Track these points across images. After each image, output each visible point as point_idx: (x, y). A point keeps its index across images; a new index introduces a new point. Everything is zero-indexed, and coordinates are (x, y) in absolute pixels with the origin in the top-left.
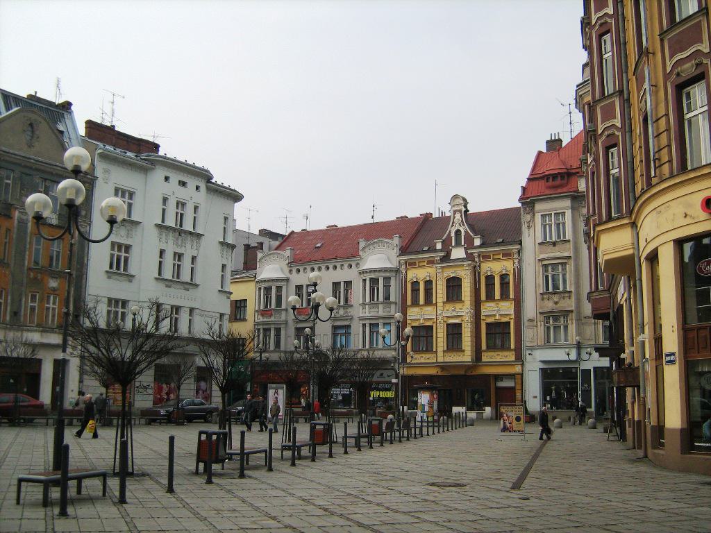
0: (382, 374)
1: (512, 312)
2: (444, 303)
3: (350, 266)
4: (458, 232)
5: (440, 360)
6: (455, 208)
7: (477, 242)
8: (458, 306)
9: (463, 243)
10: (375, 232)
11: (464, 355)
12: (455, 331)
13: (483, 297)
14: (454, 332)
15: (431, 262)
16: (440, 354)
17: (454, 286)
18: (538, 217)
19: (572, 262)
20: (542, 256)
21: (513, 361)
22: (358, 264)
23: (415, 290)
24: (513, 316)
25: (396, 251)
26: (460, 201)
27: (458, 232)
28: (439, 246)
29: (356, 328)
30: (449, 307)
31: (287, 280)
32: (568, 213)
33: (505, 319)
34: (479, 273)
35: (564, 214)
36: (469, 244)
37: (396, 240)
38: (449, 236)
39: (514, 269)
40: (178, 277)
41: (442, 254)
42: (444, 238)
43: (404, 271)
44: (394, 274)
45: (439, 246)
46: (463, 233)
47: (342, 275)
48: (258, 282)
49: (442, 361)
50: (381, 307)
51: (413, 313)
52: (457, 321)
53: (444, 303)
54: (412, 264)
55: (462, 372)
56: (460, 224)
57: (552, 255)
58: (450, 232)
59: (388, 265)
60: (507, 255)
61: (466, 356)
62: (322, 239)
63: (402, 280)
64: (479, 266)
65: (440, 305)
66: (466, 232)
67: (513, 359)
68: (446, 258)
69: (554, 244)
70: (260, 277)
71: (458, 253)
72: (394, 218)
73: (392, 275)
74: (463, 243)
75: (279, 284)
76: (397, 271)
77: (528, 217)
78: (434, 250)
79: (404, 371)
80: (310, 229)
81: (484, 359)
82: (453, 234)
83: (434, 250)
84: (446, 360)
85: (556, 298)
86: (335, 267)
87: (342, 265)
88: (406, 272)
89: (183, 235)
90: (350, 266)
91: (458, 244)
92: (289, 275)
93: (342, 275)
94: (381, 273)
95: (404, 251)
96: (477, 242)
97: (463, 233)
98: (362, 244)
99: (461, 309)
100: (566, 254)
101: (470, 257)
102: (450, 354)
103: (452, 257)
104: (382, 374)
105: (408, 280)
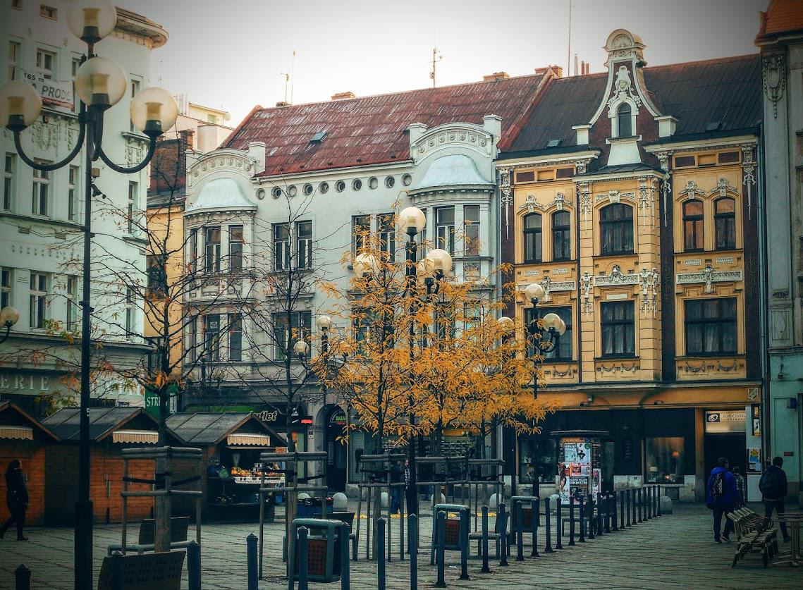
1: (741, 278)
2: (595, 258)
3: (390, 181)
4: (623, 110)
5: (588, 377)
6: (618, 59)
7: (666, 129)
8: (626, 263)
9: (634, 133)
10: (447, 108)
11: (638, 368)
12: (620, 315)
13: (679, 247)
14: (618, 320)
15: (566, 174)
16: (588, 366)
17: (617, 222)
21: (742, 380)
22: (407, 177)
23: (532, 233)
24: (741, 286)
25: (491, 149)
28: (583, 138)
30: (605, 264)
31: (253, 212)
33: (725, 293)
34: (670, 196)
36: (648, 129)
37: (493, 125)
38: (605, 119)
39: (745, 187)
40: (43, 211)
41: (592, 155)
42: (593, 121)
43: (507, 192)
44: (487, 197)
45: (583, 138)
46: (634, 112)
47: (374, 197)
48: (188, 217)
49: (593, 380)
51: (531, 284)
52: (623, 296)
53: (595, 258)
54: (527, 177)
55: (633, 403)
56: (627, 92)
58: (607, 109)
59: (473, 179)
60: (728, 158)
61: (647, 369)
62: (325, 122)
63: (503, 209)
64: (670, 181)
65: (586, 262)
66: (642, 109)
67: (742, 374)
68: (597, 166)
70: (189, 209)
71: (624, 153)
73: (481, 200)
74: (634, 133)
75: (236, 220)
76: (492, 190)
80: (295, 100)
81: (683, 375)
82: (613, 113)
84: (600, 379)
86: (358, 185)
87: (373, 179)
88: (512, 194)
89: (51, 121)
90: (390, 181)
91: (624, 134)
92: (255, 200)
93: (374, 197)
94: (458, 196)
95: (505, 152)
96: (666, 129)
97: (634, 112)
98: (416, 133)
99: (631, 271)
101: (649, 161)
102: (608, 365)
103: (610, 163)
105: (517, 210)
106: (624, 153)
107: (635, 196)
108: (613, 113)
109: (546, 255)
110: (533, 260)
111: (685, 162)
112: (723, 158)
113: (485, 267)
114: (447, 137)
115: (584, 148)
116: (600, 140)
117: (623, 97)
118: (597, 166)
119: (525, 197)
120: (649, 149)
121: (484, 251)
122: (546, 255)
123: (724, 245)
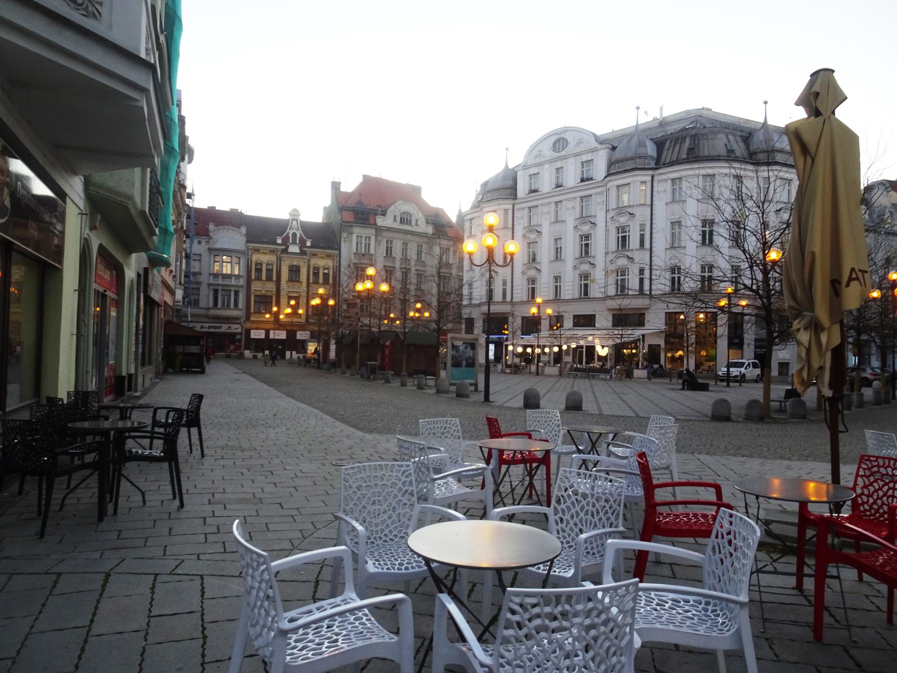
4: (294, 235)
7: (309, 244)
18: (354, 236)
23: (259, 270)
26: (295, 213)
27: (294, 235)
28: (279, 241)
29: (204, 290)
30: (290, 284)
32: (373, 238)
35: (370, 238)
36: (302, 243)
38: (287, 236)
45: (279, 241)
46: (298, 236)
54: (257, 250)
60: (329, 256)
68: (285, 251)
69: (364, 255)
72: (206, 207)
78: (275, 243)
82: (290, 235)
91: (294, 243)
96: (309, 244)
97: (298, 236)
98: (211, 227)
101: (303, 253)
103: (289, 250)
104: (229, 328)
106: (294, 249)
107: (302, 264)
108: (290, 235)
109: (264, 278)
110: (259, 278)
111: (315, 255)
117: (294, 231)
119: (255, 257)
122: (264, 278)
123: (269, 278)
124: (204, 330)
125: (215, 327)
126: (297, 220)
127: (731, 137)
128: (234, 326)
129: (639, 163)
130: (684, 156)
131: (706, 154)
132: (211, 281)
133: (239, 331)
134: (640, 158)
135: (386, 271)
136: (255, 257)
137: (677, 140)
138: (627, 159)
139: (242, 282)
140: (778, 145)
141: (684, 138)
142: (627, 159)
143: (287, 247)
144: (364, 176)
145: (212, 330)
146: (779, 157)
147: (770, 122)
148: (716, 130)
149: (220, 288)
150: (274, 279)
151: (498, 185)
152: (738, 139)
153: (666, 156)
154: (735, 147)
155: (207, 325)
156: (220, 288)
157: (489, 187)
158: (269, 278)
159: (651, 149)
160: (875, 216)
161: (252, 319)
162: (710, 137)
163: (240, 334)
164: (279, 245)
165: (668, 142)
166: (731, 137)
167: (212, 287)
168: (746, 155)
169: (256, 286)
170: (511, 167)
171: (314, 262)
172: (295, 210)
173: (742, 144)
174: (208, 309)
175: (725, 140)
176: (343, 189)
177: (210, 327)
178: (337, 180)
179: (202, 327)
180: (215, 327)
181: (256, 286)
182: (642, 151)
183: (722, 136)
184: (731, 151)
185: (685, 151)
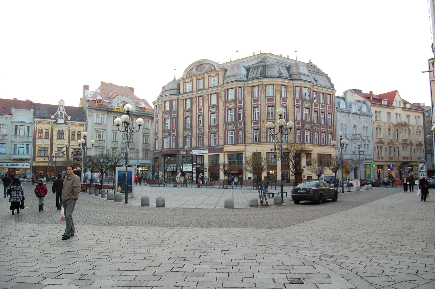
0: (23, 165)
4: (61, 114)
13: (71, 139)
19: (106, 131)
20: (96, 128)
27: (61, 114)
28: (53, 117)
29: (9, 144)
30: (59, 141)
36: (66, 118)
38: (57, 115)
45: (53, 117)
46: (63, 114)
50: (26, 138)
54: (40, 122)
57: (100, 128)
58: (58, 113)
66: (65, 114)
68: (56, 123)
69: (100, 124)
71: (61, 121)
77: (90, 113)
78: (50, 118)
79: (34, 164)
82: (59, 114)
83: (50, 118)
85: (100, 142)
91: (61, 118)
97: (63, 114)
98: (14, 110)
100: (104, 128)
101: (66, 123)
106: (61, 121)
108: (59, 114)
109: (43, 137)
110: (40, 138)
112: (80, 125)
113: (30, 138)
114: (22, 112)
115: (53, 119)
116: (56, 118)
117: (61, 111)
118: (56, 123)
119: (39, 126)
120: (66, 121)
121: (30, 135)
122: (43, 137)
124: (8, 167)
125: (14, 165)
126: (63, 106)
127: (280, 67)
128: (25, 164)
129: (238, 78)
130: (259, 75)
131: (269, 75)
132: (13, 140)
133: (29, 167)
134: (238, 75)
135: (113, 133)
136: (39, 126)
137: (256, 67)
138: (232, 76)
139: (31, 140)
140: (302, 71)
141: (259, 67)
142: (232, 76)
143: (57, 120)
144: (102, 82)
145: (13, 167)
146: (303, 77)
147: (298, 60)
148: (273, 63)
149: (18, 143)
150: (50, 138)
151: (170, 87)
152: (284, 68)
153: (251, 75)
154: (282, 72)
155: (10, 164)
156: (18, 143)
157: (166, 89)
158: (46, 138)
159: (244, 72)
160: (348, 106)
161: (36, 160)
162: (270, 66)
163: (30, 168)
164: (53, 119)
165: (252, 68)
166: (280, 67)
167: (13, 143)
168: (288, 76)
169: (39, 142)
170: (177, 79)
171: (73, 128)
172: (62, 100)
173: (286, 71)
174: (11, 155)
175: (278, 69)
176: (90, 89)
177: (11, 165)
178: (87, 84)
179: (7, 165)
180: (14, 165)
181: (39, 142)
182: (239, 72)
183: (276, 66)
184: (280, 74)
185: (259, 73)
